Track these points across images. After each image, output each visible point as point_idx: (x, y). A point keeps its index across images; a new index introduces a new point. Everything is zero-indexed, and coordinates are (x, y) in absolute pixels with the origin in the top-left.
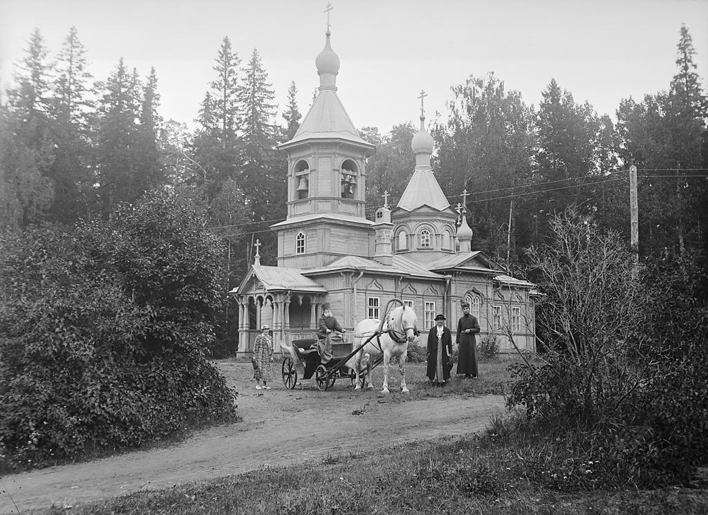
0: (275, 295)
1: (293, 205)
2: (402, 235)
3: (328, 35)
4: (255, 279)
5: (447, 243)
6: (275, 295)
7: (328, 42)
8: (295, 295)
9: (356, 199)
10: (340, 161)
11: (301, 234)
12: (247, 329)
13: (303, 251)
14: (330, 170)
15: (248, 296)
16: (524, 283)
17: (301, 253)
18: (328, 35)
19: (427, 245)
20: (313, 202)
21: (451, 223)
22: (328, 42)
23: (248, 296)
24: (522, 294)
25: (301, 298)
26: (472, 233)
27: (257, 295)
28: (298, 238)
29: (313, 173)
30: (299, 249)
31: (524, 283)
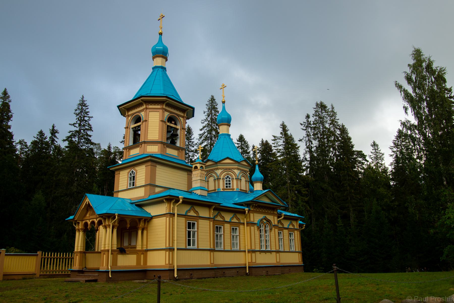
0: (105, 219)
1: (128, 150)
2: (211, 179)
3: (161, 34)
4: (89, 207)
5: (244, 185)
6: (105, 219)
7: (160, 40)
8: (122, 219)
9: (178, 144)
10: (167, 114)
11: (132, 172)
12: (82, 250)
13: (133, 185)
14: (158, 121)
15: (84, 222)
16: (296, 215)
17: (132, 187)
18: (161, 34)
19: (229, 187)
20: (143, 145)
21: (246, 171)
22: (160, 40)
23: (84, 222)
24: (294, 223)
26: (262, 176)
27: (91, 220)
28: (131, 174)
29: (144, 123)
30: (130, 184)
31: (296, 215)
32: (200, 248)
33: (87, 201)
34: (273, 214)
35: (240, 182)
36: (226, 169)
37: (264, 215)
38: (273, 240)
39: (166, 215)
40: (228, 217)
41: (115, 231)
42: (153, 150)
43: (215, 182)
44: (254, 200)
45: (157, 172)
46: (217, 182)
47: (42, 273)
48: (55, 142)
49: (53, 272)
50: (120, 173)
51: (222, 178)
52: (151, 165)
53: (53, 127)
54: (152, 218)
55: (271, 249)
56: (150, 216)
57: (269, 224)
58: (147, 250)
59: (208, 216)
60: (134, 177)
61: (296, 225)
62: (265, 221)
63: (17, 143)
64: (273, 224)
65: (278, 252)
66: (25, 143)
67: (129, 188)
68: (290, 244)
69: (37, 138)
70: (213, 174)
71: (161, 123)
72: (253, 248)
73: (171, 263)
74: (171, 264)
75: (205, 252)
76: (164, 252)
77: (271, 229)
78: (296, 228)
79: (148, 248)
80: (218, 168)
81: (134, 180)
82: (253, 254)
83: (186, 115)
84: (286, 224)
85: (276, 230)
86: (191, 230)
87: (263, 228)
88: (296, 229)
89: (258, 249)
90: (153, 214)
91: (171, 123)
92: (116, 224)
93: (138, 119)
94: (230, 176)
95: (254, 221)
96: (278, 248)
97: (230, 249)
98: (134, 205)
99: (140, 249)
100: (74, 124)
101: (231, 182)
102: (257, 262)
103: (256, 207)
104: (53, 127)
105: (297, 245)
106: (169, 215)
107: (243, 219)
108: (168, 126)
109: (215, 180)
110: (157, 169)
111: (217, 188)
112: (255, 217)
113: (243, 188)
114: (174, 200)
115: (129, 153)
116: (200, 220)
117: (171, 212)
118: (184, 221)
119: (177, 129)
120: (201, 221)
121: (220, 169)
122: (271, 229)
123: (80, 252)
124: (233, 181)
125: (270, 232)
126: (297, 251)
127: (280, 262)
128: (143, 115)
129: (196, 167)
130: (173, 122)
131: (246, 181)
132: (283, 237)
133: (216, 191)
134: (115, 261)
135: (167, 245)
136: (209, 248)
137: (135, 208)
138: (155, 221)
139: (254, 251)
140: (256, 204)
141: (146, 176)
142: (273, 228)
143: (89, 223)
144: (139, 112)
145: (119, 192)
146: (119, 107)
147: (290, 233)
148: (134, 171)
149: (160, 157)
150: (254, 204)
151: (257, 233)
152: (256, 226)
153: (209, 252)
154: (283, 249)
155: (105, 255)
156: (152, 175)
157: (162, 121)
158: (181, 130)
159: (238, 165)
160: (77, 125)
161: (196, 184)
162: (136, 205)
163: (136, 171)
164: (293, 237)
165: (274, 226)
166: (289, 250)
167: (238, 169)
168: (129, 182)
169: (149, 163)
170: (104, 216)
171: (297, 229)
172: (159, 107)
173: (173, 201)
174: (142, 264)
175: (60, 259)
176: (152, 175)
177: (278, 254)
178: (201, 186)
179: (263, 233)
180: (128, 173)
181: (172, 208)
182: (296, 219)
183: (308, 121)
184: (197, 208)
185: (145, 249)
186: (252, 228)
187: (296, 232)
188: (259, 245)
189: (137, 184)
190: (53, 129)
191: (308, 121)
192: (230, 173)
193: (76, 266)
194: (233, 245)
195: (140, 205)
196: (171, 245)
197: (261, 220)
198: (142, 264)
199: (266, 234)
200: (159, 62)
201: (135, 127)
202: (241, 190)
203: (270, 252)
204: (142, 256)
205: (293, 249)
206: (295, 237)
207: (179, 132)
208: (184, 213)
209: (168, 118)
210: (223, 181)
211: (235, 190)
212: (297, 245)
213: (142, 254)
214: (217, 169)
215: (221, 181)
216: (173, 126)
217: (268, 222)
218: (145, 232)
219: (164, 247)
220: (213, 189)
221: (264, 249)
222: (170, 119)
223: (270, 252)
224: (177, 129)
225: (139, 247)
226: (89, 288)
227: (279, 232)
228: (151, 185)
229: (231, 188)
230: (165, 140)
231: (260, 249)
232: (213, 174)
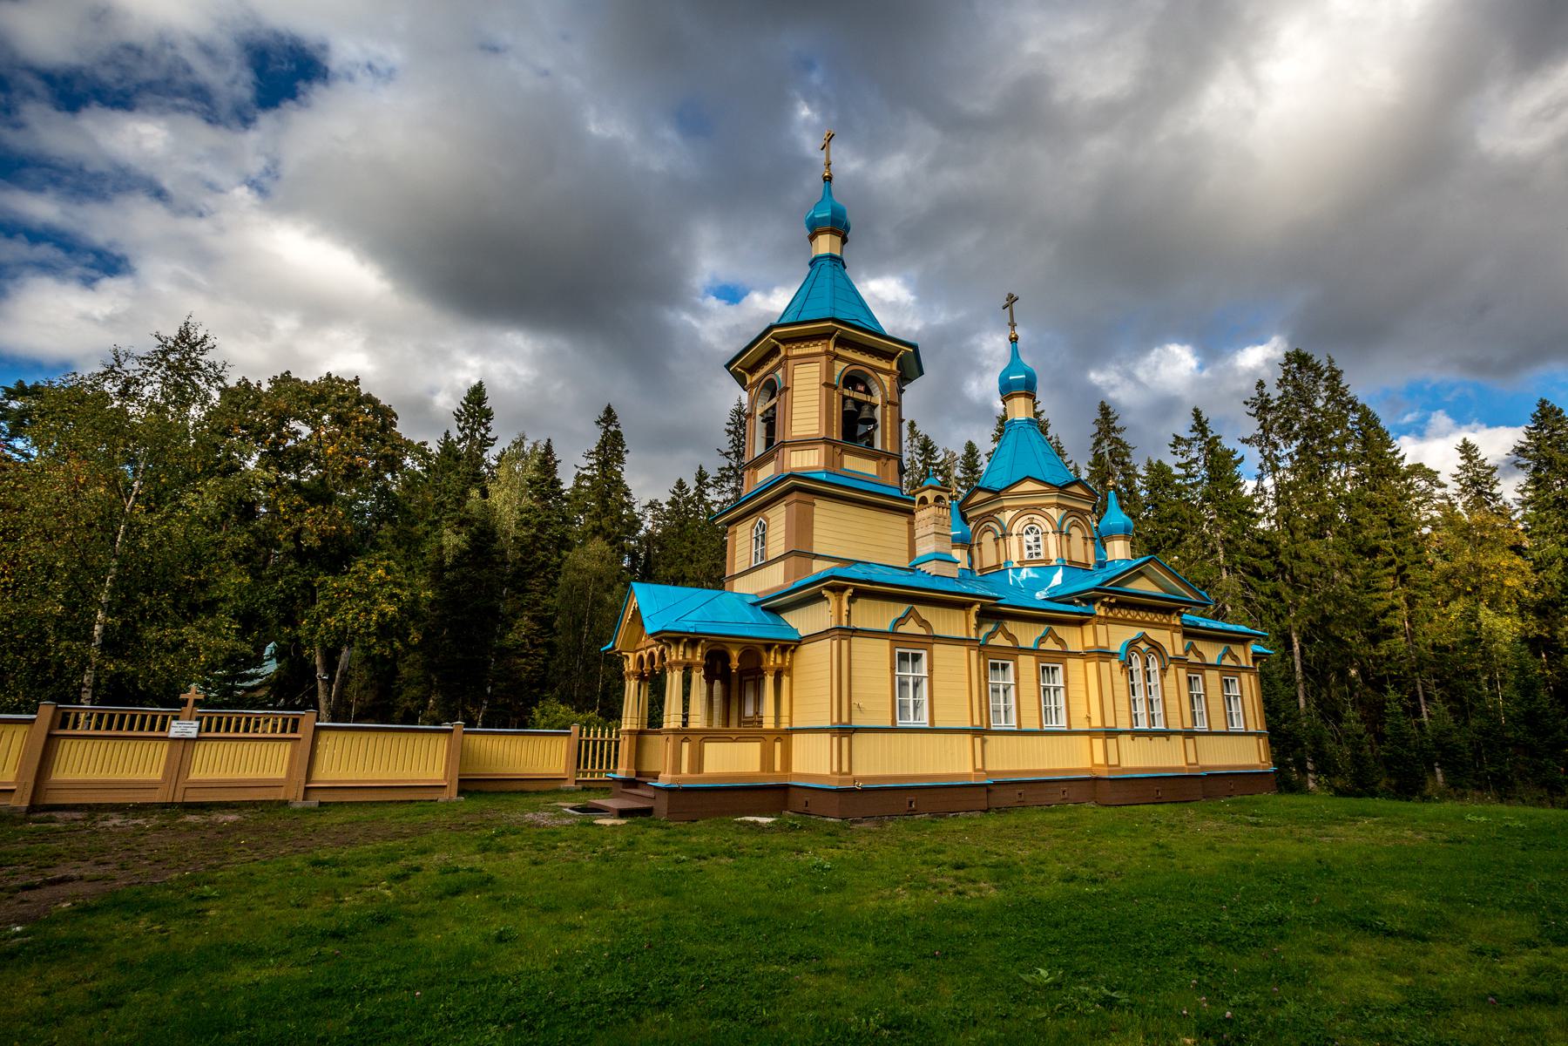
9: (878, 446)
12: (635, 727)
15: (638, 654)
16: (1243, 628)
17: (759, 563)
23: (638, 654)
24: (1237, 650)
25: (735, 654)
32: (938, 725)
33: (635, 601)
35: (1069, 541)
36: (1026, 507)
37: (1143, 630)
38: (1172, 701)
39: (831, 634)
40: (1027, 635)
41: (698, 677)
42: (808, 460)
43: (997, 545)
44: (1106, 586)
45: (816, 517)
46: (1001, 541)
47: (581, 778)
48: (706, 497)
49: (592, 775)
50: (735, 532)
51: (1014, 531)
52: (797, 501)
53: (701, 467)
54: (800, 642)
55: (1167, 725)
56: (797, 638)
57: (1157, 653)
58: (791, 731)
60: (763, 536)
61: (1244, 654)
62: (1143, 646)
63: (646, 507)
64: (1171, 655)
65: (1189, 734)
66: (661, 505)
67: (753, 565)
68: (1228, 711)
69: (674, 493)
70: (992, 525)
71: (824, 388)
72: (1110, 723)
73: (845, 769)
74: (845, 774)
76: (828, 735)
77: (1164, 670)
78: (1244, 664)
79: (795, 725)
80: (1003, 507)
81: (763, 544)
82: (1111, 742)
83: (894, 368)
84: (1212, 653)
85: (1182, 672)
87: (1137, 665)
88: (1245, 669)
89: (1124, 725)
90: (803, 633)
91: (854, 389)
92: (698, 659)
93: (771, 389)
94: (1037, 527)
95: (1108, 648)
96: (1188, 724)
97: (1037, 728)
98: (759, 608)
99: (772, 726)
100: (727, 454)
101: (1041, 542)
102: (1124, 765)
103: (1111, 606)
104: (701, 467)
105: (1250, 714)
106: (837, 632)
107: (1075, 639)
108: (845, 398)
109: (996, 539)
110: (816, 510)
111: (1002, 561)
113: (1078, 556)
114: (851, 590)
115: (755, 480)
116: (936, 647)
117: (844, 624)
118: (888, 648)
119: (874, 406)
120: (938, 649)
121: (1010, 508)
122: (1164, 670)
123: (630, 732)
125: (1161, 677)
126: (1252, 729)
127: (1196, 764)
128: (780, 376)
129: (924, 501)
130: (861, 388)
131: (1085, 538)
132: (1205, 690)
133: (1002, 568)
134: (698, 761)
135: (835, 720)
137: (752, 616)
138: (806, 649)
140: (1111, 598)
141: (787, 530)
142: (1172, 666)
143: (645, 657)
144: (772, 371)
145: (734, 577)
146: (728, 366)
147: (1226, 681)
148: (764, 522)
149: (824, 477)
150: (1104, 597)
151: (1121, 680)
152: (1115, 663)
153: (968, 737)
154: (1206, 726)
156: (802, 528)
157: (827, 385)
158: (884, 407)
160: (732, 456)
161: (925, 548)
162: (763, 609)
163: (767, 519)
164: (1235, 691)
165: (1171, 658)
166: (1227, 728)
167: (1059, 506)
168: (754, 551)
169: (794, 496)
170: (666, 638)
171: (1247, 668)
172: (819, 349)
173: (849, 592)
174: (778, 767)
175: (602, 743)
176: (802, 528)
177: (1190, 742)
178: (939, 550)
179: (1139, 679)
180: (753, 527)
181: (845, 613)
182: (1242, 640)
183: (1262, 395)
184: (924, 612)
185: (785, 725)
186: (1104, 666)
187: (1244, 676)
188: (1127, 714)
189: (769, 553)
190: (700, 473)
191: (1262, 395)
192: (1035, 516)
193: (622, 771)
194: (1044, 713)
195: (774, 607)
196: (845, 719)
197: (1132, 644)
198: (778, 767)
199: (1148, 684)
200: (825, 245)
201: (766, 411)
202: (1070, 561)
203: (1166, 734)
204: (778, 745)
205: (1238, 726)
206: (1241, 692)
207: (878, 413)
208: (887, 627)
209: (843, 377)
211: (1054, 563)
212: (1250, 714)
213: (775, 741)
214: (1002, 509)
215: (1014, 541)
216: (863, 397)
217: (1154, 650)
218: (785, 680)
219: (828, 724)
220: (994, 563)
221: (1143, 725)
222: (851, 380)
223: (1166, 734)
224: (874, 406)
225: (769, 723)
227: (1190, 678)
228: (800, 553)
229: (1042, 557)
230: (836, 435)
232: (992, 525)
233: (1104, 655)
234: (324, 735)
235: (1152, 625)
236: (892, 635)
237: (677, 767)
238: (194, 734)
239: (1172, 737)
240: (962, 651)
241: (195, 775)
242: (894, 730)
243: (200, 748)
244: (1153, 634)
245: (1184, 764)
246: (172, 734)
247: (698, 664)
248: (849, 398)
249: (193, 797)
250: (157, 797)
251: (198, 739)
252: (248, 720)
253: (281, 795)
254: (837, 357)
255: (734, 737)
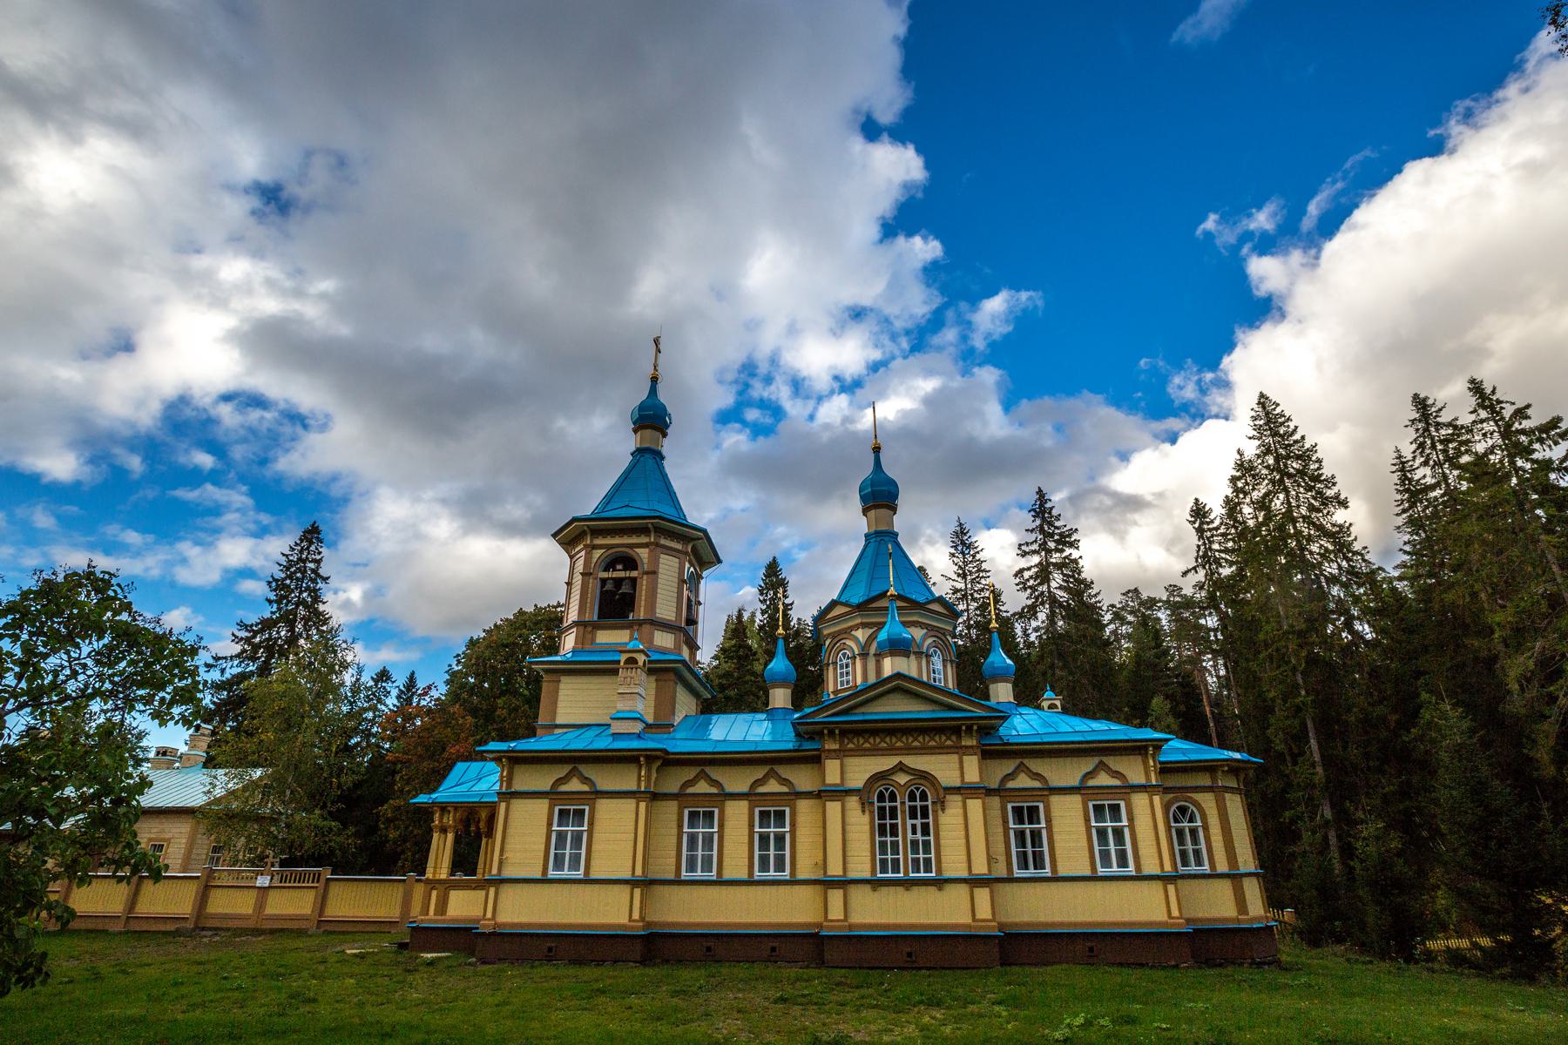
32: (594, 875)
34: (961, 750)
40: (737, 781)
59: (634, 787)
75: (616, 888)
86: (570, 828)
91: (615, 570)
108: (604, 581)
110: (562, 686)
112: (848, 769)
124: (854, 664)
136: (627, 875)
139: (844, 883)
153: (626, 889)
155: (434, 893)
159: (862, 616)
187: (1140, 801)
210: (835, 669)
223: (940, 883)
226: (200, 963)
231: (873, 871)
233: (840, 793)
234: (332, 884)
235: (909, 750)
236: (552, 795)
237: (425, 911)
238: (267, 885)
239: (949, 888)
240: (630, 804)
241: (266, 912)
242: (678, 882)
243: (272, 893)
244: (912, 761)
245: (970, 921)
246: (258, 885)
247: (450, 826)
248: (608, 578)
249: (267, 925)
250: (251, 924)
251: (270, 887)
252: (314, 875)
253: (303, 925)
254: (595, 547)
255: (474, 885)
